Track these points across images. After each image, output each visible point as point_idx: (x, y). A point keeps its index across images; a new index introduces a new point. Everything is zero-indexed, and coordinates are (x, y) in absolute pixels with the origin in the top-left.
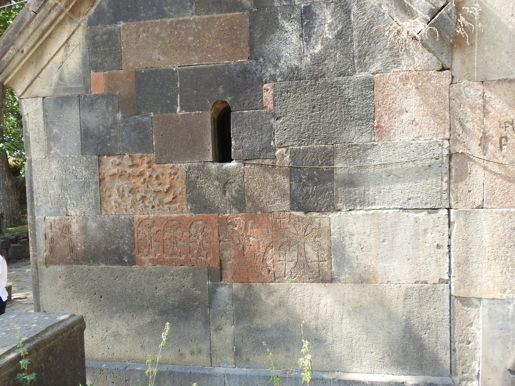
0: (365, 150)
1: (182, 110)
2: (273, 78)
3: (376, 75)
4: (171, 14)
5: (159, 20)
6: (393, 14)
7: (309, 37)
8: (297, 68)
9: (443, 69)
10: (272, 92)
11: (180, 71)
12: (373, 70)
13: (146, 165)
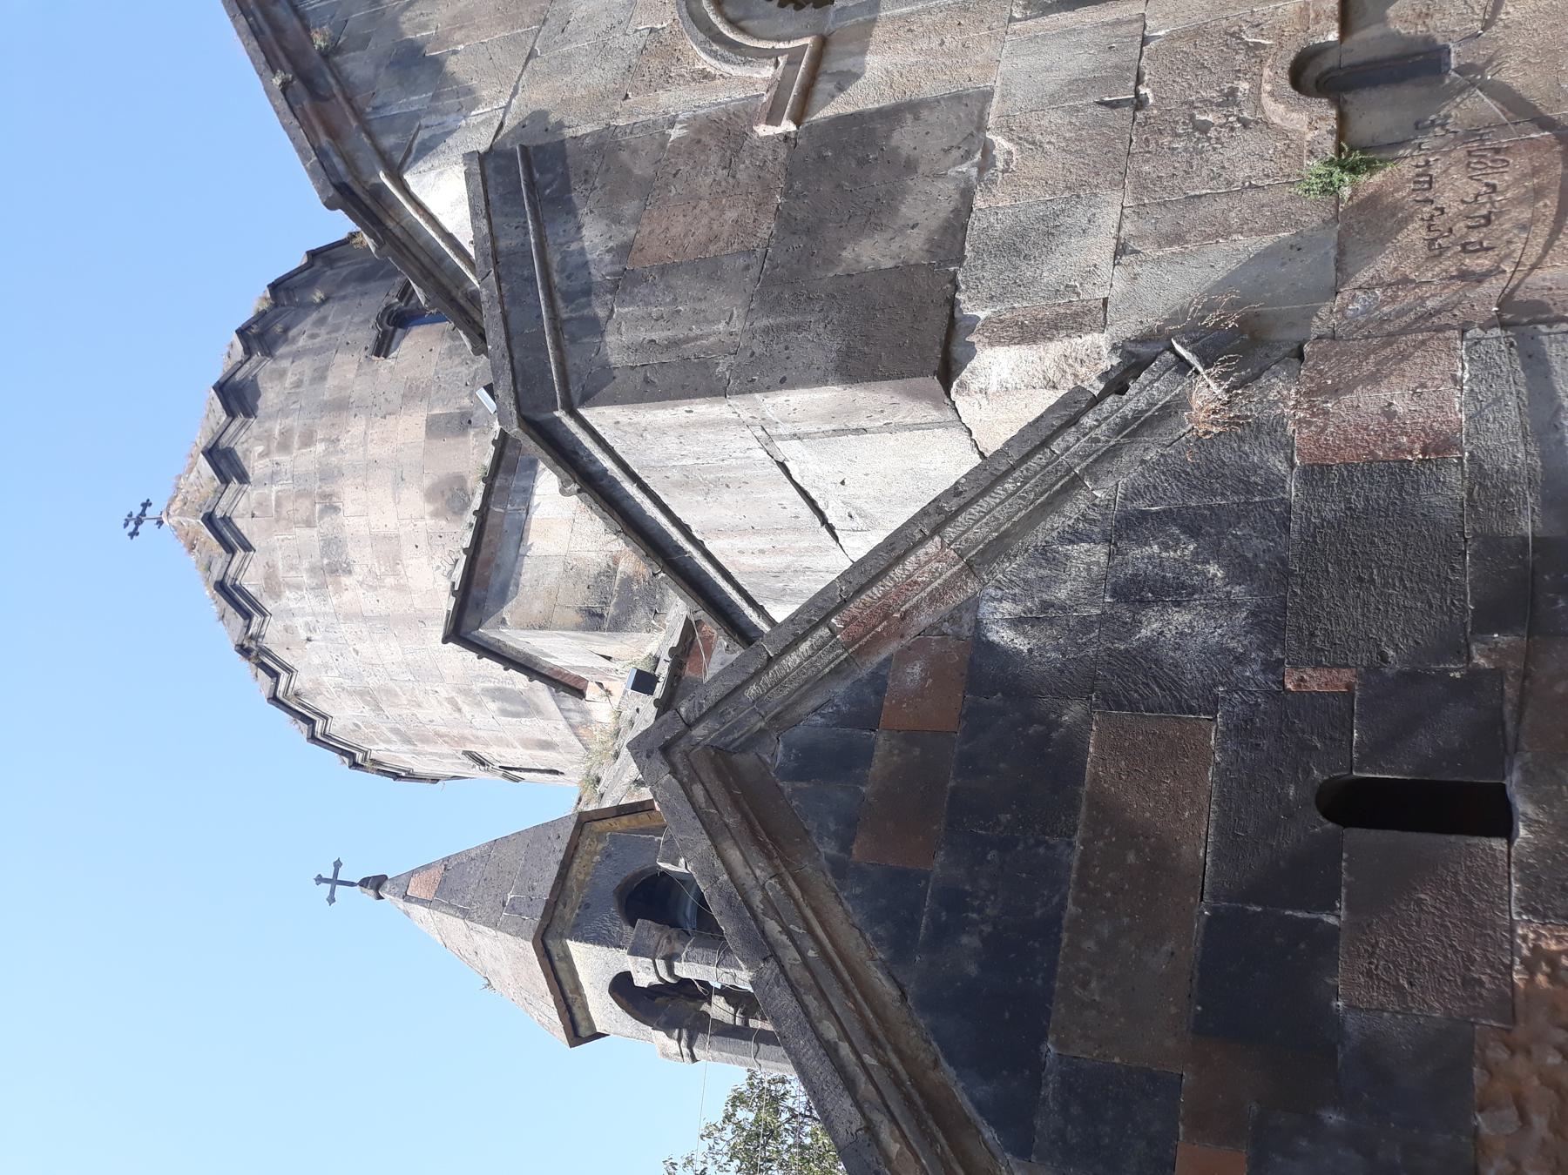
0: (1485, 476)
1: (1331, 909)
2: (1273, 667)
3: (1297, 461)
4: (1056, 899)
5: (1065, 936)
6: (1167, 440)
7: (1183, 586)
8: (1252, 614)
9: (1300, 356)
10: (1309, 671)
11: (1214, 897)
12: (1283, 468)
13: (1520, 1066)
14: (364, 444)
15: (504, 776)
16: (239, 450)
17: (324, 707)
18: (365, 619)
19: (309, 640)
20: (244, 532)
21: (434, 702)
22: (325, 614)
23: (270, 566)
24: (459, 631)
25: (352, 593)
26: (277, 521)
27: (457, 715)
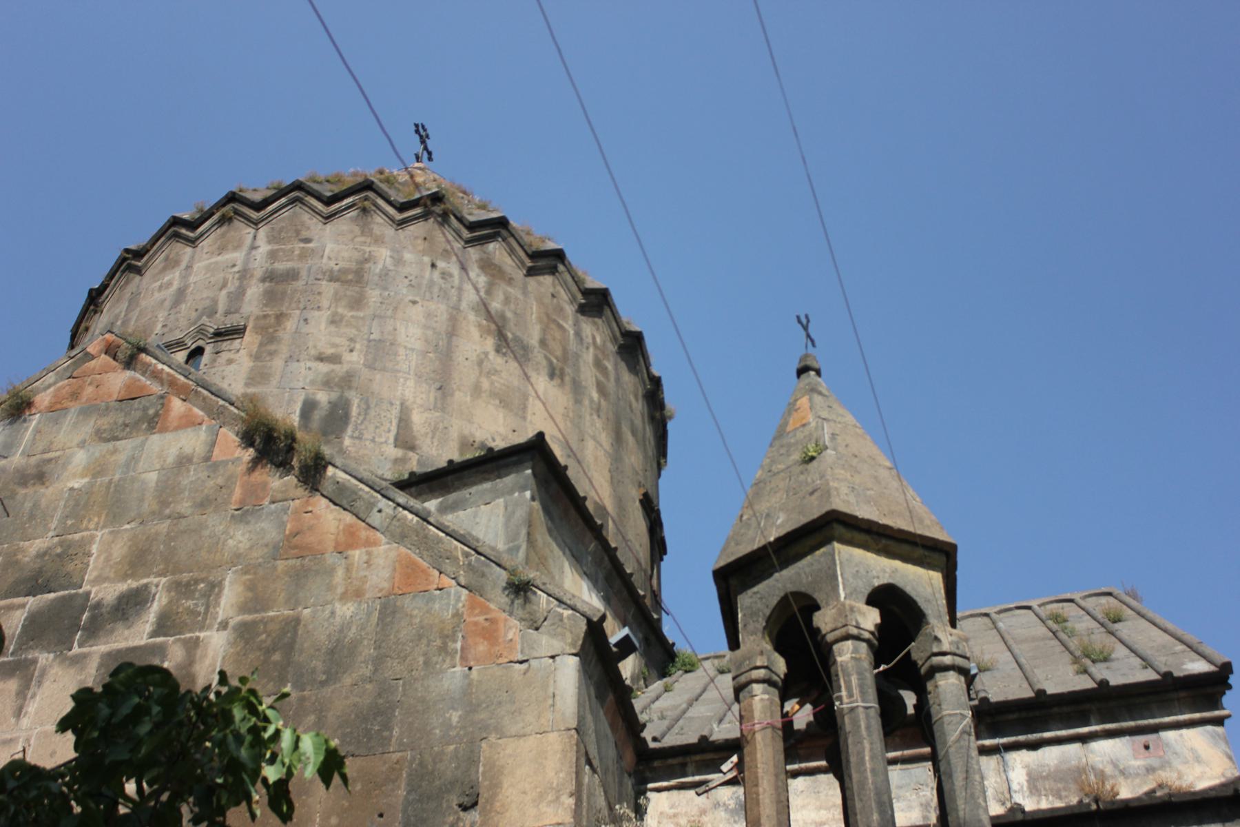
14: (594, 438)
15: (179, 344)
16: (599, 321)
17: (345, 224)
18: (452, 332)
19: (433, 266)
20: (541, 278)
21: (337, 340)
22: (460, 300)
23: (510, 281)
24: (535, 452)
25: (474, 343)
26: (548, 315)
27: (313, 352)
